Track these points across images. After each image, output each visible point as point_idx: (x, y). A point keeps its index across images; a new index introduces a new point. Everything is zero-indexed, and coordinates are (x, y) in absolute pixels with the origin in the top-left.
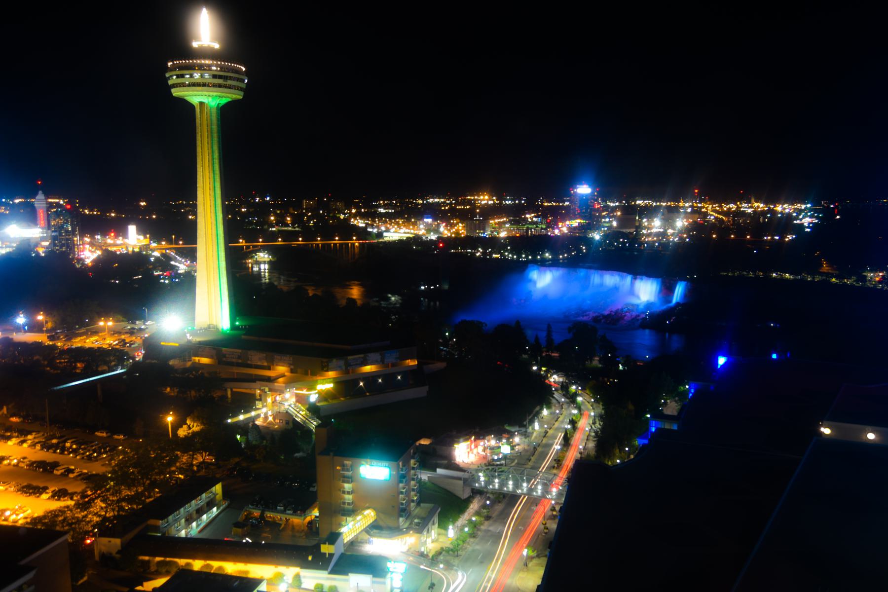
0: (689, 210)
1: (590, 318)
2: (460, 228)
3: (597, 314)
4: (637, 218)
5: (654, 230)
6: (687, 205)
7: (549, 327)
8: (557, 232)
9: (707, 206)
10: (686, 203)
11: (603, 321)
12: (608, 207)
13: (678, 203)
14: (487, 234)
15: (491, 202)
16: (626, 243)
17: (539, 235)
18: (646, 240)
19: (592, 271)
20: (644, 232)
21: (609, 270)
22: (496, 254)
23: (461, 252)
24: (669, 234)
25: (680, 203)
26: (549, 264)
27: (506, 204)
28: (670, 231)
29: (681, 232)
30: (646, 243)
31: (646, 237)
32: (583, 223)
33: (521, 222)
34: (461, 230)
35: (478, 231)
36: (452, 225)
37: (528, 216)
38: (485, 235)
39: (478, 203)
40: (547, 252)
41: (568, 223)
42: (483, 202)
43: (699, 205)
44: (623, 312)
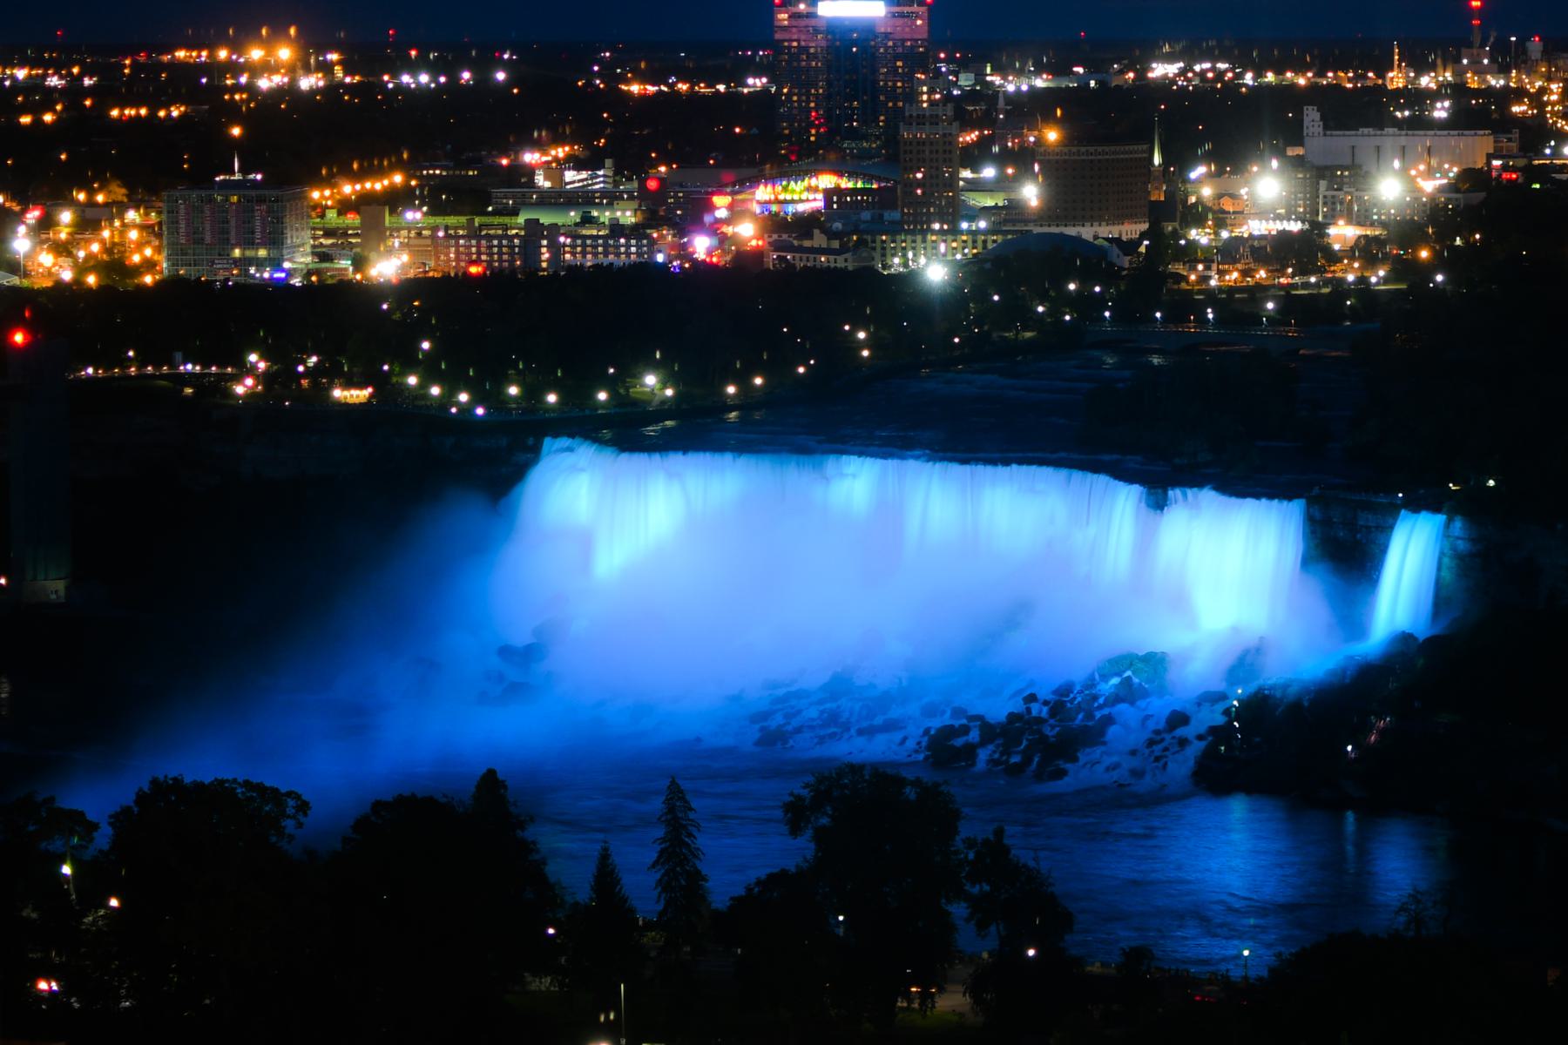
0: (1441, 111)
1: (910, 744)
2: (134, 235)
3: (946, 720)
4: (1157, 159)
5: (1257, 227)
6: (1426, 81)
7: (676, 797)
8: (701, 245)
9: (1538, 84)
10: (1421, 68)
12: (989, 96)
13: (1381, 74)
14: (297, 262)
15: (307, 83)
16: (1100, 302)
17: (595, 266)
18: (1213, 283)
19: (912, 465)
20: (1200, 236)
21: (1007, 462)
22: (349, 384)
23: (141, 377)
24: (1337, 247)
25: (1391, 75)
26: (665, 430)
27: (400, 88)
28: (1342, 233)
29: (1407, 231)
30: (1212, 297)
31: (1208, 263)
32: (854, 192)
33: (497, 192)
34: (140, 246)
35: (237, 253)
36: (88, 223)
37: (530, 157)
38: (283, 275)
39: (237, 88)
40: (654, 366)
41: (763, 193)
42: (264, 84)
43: (1496, 82)
44: (1095, 698)
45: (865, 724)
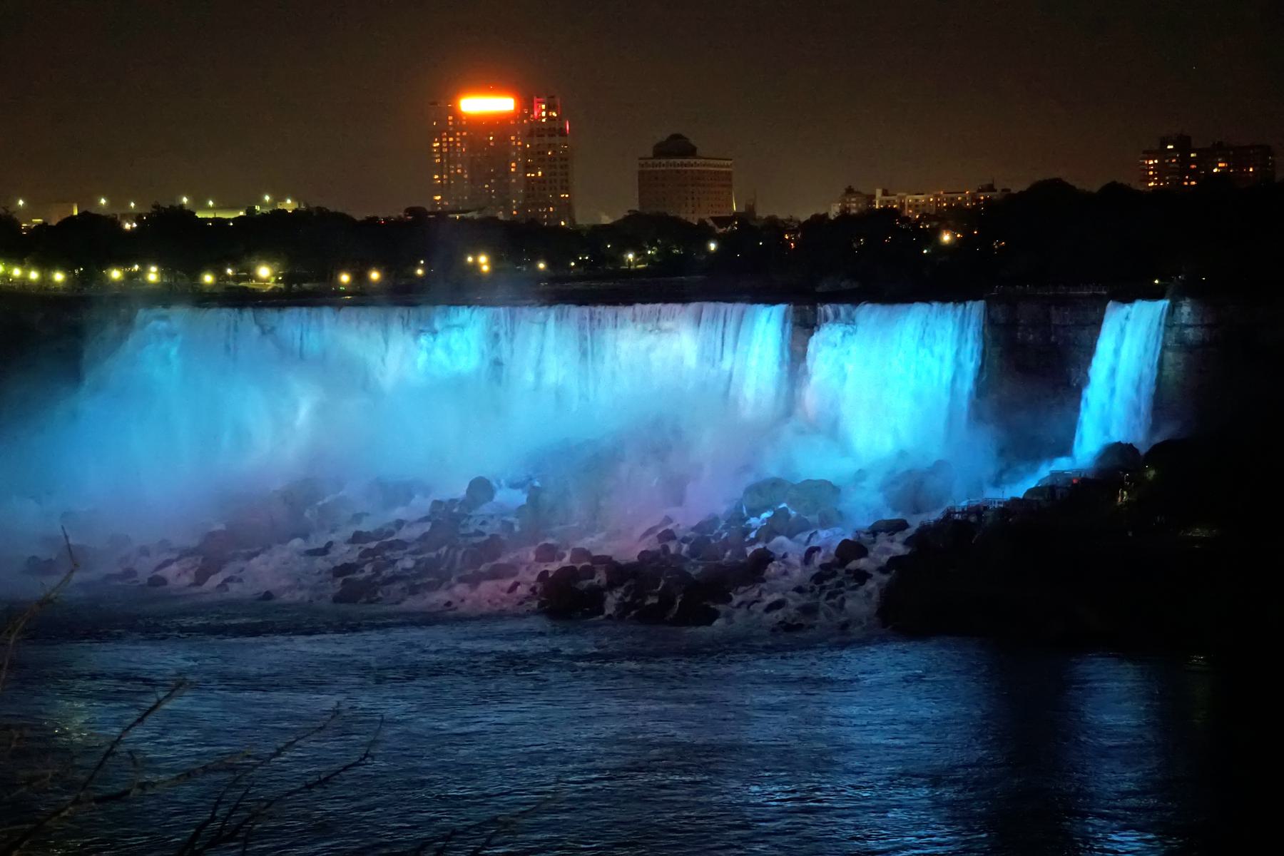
1: (522, 591)
11: (611, 601)
44: (746, 532)
45: (469, 572)
